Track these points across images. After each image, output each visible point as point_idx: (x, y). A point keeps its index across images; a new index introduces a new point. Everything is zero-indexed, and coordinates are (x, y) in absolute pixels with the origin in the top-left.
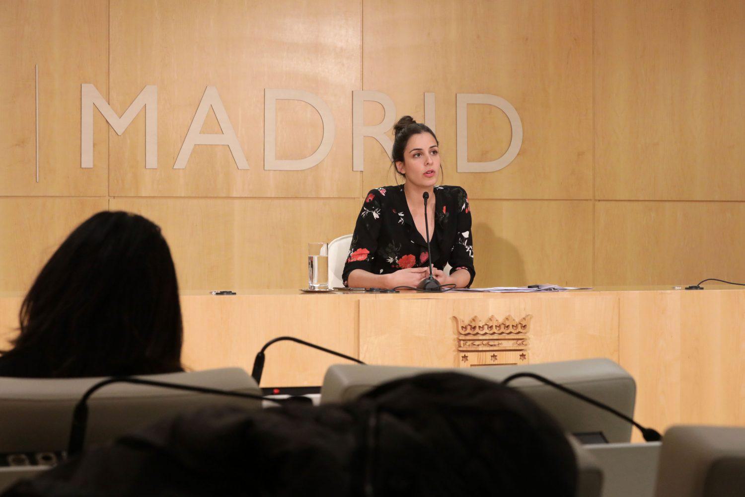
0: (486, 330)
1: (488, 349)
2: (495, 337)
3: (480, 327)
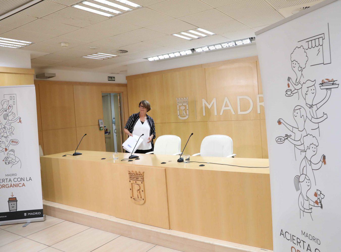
0: (134, 175)
1: (134, 180)
2: (136, 177)
3: (133, 174)
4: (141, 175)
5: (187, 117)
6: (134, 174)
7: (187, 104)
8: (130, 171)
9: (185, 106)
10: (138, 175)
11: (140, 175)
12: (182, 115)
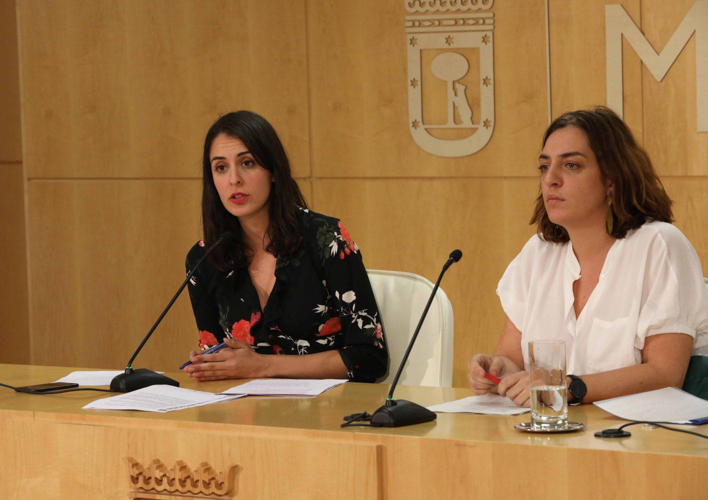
3: (159, 482)
4: (219, 486)
5: (483, 135)
6: (171, 482)
7: (485, 40)
8: (139, 461)
9: (470, 55)
10: (195, 484)
11: (207, 485)
12: (445, 121)
